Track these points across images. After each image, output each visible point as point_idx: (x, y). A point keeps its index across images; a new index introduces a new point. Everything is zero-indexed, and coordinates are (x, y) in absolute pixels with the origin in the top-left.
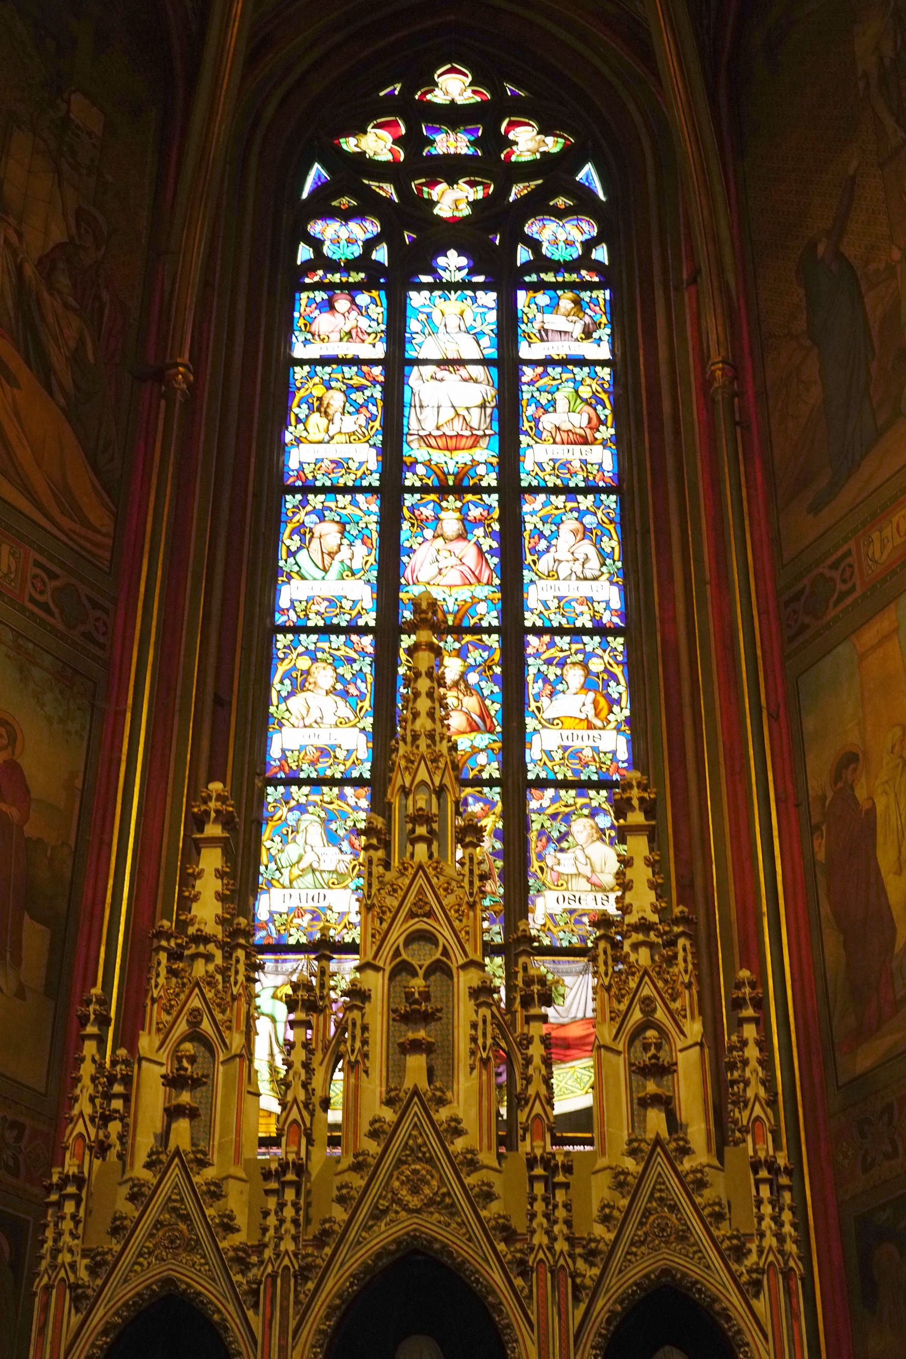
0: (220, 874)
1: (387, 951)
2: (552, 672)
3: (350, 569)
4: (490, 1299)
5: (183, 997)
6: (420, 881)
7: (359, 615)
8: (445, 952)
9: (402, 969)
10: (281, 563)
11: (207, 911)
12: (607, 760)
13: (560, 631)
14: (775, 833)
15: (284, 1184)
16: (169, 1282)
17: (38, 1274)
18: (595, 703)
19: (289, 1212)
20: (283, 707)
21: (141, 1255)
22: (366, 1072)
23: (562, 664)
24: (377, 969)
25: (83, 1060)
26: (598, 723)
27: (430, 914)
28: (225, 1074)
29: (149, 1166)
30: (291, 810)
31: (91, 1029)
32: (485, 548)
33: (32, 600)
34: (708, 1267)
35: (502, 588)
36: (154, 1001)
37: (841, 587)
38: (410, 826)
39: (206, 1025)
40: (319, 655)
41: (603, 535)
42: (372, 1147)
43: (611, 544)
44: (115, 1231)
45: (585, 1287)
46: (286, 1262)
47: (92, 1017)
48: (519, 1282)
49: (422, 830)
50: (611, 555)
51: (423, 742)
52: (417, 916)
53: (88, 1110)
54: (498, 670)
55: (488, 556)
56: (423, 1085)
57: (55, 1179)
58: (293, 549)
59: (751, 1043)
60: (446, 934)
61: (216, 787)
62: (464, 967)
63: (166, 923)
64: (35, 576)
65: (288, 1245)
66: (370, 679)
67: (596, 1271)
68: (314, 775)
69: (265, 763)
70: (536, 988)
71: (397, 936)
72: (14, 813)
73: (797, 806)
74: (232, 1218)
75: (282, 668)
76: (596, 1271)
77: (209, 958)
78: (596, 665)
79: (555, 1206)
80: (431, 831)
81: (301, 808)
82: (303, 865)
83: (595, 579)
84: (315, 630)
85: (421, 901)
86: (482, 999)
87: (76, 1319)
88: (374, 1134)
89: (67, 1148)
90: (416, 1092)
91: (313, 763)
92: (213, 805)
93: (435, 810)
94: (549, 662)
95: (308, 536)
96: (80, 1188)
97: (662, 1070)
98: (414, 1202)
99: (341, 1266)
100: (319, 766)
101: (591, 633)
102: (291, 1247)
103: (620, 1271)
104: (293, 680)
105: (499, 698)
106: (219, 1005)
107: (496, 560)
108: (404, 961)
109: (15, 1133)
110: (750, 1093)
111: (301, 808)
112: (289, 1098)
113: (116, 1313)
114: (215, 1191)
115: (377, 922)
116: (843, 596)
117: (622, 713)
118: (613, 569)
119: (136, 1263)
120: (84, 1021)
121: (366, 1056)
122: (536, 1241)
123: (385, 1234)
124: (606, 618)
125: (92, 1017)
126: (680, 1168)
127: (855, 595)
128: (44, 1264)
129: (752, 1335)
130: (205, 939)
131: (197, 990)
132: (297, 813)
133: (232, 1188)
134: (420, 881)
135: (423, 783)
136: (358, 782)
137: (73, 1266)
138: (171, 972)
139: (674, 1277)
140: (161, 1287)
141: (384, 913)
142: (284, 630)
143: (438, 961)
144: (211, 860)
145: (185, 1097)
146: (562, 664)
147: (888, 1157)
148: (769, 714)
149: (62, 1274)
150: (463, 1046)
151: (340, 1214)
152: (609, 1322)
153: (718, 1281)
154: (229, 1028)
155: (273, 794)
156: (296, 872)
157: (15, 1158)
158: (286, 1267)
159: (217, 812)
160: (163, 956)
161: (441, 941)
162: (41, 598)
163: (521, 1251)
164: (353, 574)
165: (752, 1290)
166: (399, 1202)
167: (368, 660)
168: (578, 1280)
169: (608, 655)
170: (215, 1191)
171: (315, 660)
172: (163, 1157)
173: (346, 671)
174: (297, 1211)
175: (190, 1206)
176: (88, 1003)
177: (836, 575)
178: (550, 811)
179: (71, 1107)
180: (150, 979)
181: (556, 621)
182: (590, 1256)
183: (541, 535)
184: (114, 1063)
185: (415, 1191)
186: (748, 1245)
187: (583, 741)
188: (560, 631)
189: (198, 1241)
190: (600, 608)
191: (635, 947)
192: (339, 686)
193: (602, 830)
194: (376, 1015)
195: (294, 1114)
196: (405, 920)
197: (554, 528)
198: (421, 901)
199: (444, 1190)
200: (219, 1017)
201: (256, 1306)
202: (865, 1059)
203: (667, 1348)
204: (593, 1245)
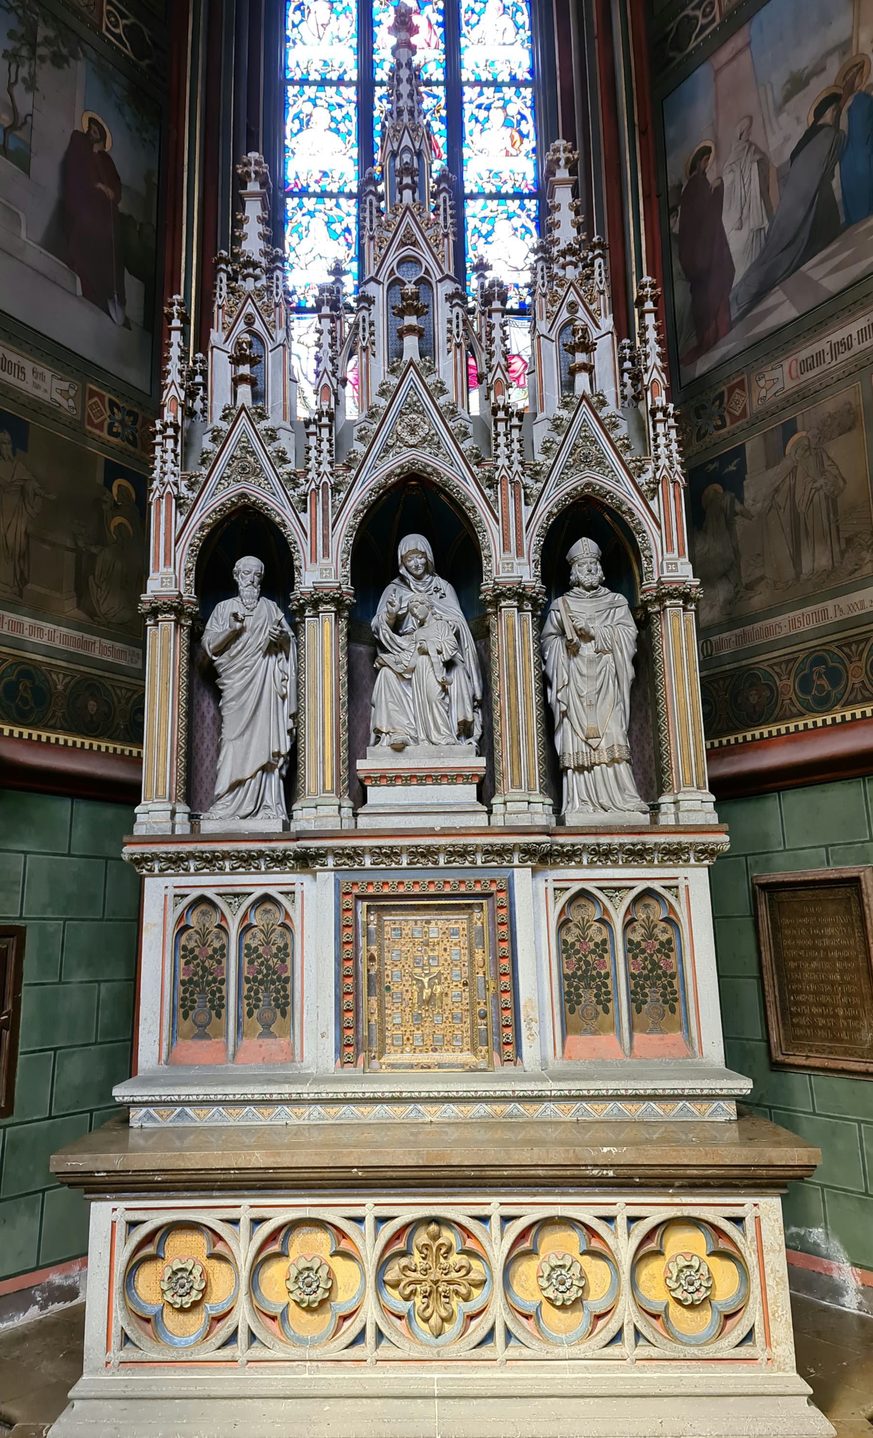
0: (261, 220)
1: (385, 271)
2: (482, 114)
3: (338, 37)
4: (467, 504)
5: (240, 305)
6: (408, 219)
7: (345, 72)
8: (427, 272)
9: (396, 283)
10: (288, 33)
11: (253, 245)
12: (519, 178)
13: (487, 84)
14: (642, 217)
15: (320, 427)
16: (243, 495)
17: (151, 491)
18: (512, 137)
19: (325, 446)
20: (295, 139)
21: (222, 478)
22: (374, 355)
23: (488, 108)
24: (379, 283)
25: (171, 345)
26: (514, 152)
27: (415, 244)
28: (273, 357)
29: (224, 418)
30: (303, 215)
31: (176, 323)
32: (433, 22)
33: (108, 29)
34: (618, 481)
35: (446, 52)
36: (219, 307)
37: (702, 21)
38: (398, 179)
39: (258, 326)
40: (318, 102)
41: (517, 11)
42: (383, 403)
43: (523, 18)
44: (203, 462)
45: (532, 496)
46: (325, 479)
47: (176, 315)
48: (487, 491)
49: (407, 180)
50: (523, 26)
51: (406, 117)
52: (406, 245)
53: (178, 380)
54: (444, 113)
55: (435, 27)
56: (417, 358)
57: (159, 427)
58: (296, 23)
59: (651, 328)
60: (427, 258)
61: (253, 155)
62: (440, 281)
63: (225, 253)
64: (109, 12)
65: (326, 468)
66: (355, 119)
67: (540, 485)
68: (318, 190)
69: (285, 183)
70: (496, 289)
71: (392, 260)
72: (110, 193)
73: (658, 196)
74: (284, 453)
75: (292, 111)
76: (540, 485)
77: (257, 278)
78: (512, 110)
79: (512, 441)
80: (413, 182)
81: (311, 214)
82: (314, 253)
83: (512, 44)
84: (315, 83)
85: (409, 235)
86: (454, 302)
87: (181, 519)
88: (382, 393)
89: (164, 406)
90: (411, 363)
91: (317, 182)
92: (252, 168)
93: (416, 165)
94: (479, 107)
95: (306, 12)
96: (176, 432)
97: (588, 347)
98: (412, 441)
99: (363, 483)
100: (321, 183)
101: (509, 85)
102: (328, 469)
103: (557, 485)
104: (301, 121)
105: (445, 133)
106: (266, 311)
107: (441, 30)
108: (397, 279)
109: (132, 418)
110: (649, 363)
111: (311, 214)
112: (321, 369)
113: (208, 517)
114: (272, 435)
115: (377, 249)
116: (704, 28)
117: (530, 144)
118: (525, 37)
119: (220, 483)
120: (170, 317)
121: (373, 343)
122: (500, 462)
123: (392, 463)
124: (523, 74)
125: (176, 315)
126: (600, 415)
127: (715, 25)
128: (156, 484)
129: (648, 525)
130: (255, 265)
131: (250, 301)
132: (308, 218)
133: (281, 434)
134: (408, 219)
135: (407, 148)
136: (350, 196)
137: (176, 484)
138: (232, 291)
139: (594, 490)
140: (239, 500)
141: (382, 242)
142: (293, 82)
143: (422, 278)
144: (253, 210)
145: (245, 369)
146: (488, 108)
147: (718, 428)
148: (641, 133)
149: (169, 489)
150: (441, 335)
151: (360, 448)
152: (548, 519)
153: (623, 490)
154: (274, 327)
155: (291, 203)
156: (310, 257)
157: (133, 435)
158: (325, 483)
159: (256, 172)
160: (223, 276)
161: (424, 263)
162: (117, 31)
163: (489, 471)
164: (340, 41)
165: (650, 495)
166: (401, 440)
167: (353, 105)
168: (528, 491)
169: (521, 102)
170: (272, 435)
171: (315, 105)
172: (233, 411)
173: (338, 114)
174: (331, 445)
175: (256, 445)
176: (172, 305)
177: (699, 13)
178: (482, 214)
179: (165, 378)
180: (215, 286)
181: (485, 76)
182: (535, 475)
183: (473, 12)
184: (195, 362)
185: (413, 432)
186: (647, 466)
187: (505, 165)
188: (487, 84)
189: (262, 470)
190: (515, 66)
191: (563, 267)
192: (333, 125)
193: (516, 230)
194: (379, 314)
195: (325, 380)
196: (397, 249)
197: (482, 5)
198: (409, 235)
199: (433, 432)
200: (266, 319)
201: (305, 511)
202: (702, 366)
203: (584, 538)
204: (538, 468)
